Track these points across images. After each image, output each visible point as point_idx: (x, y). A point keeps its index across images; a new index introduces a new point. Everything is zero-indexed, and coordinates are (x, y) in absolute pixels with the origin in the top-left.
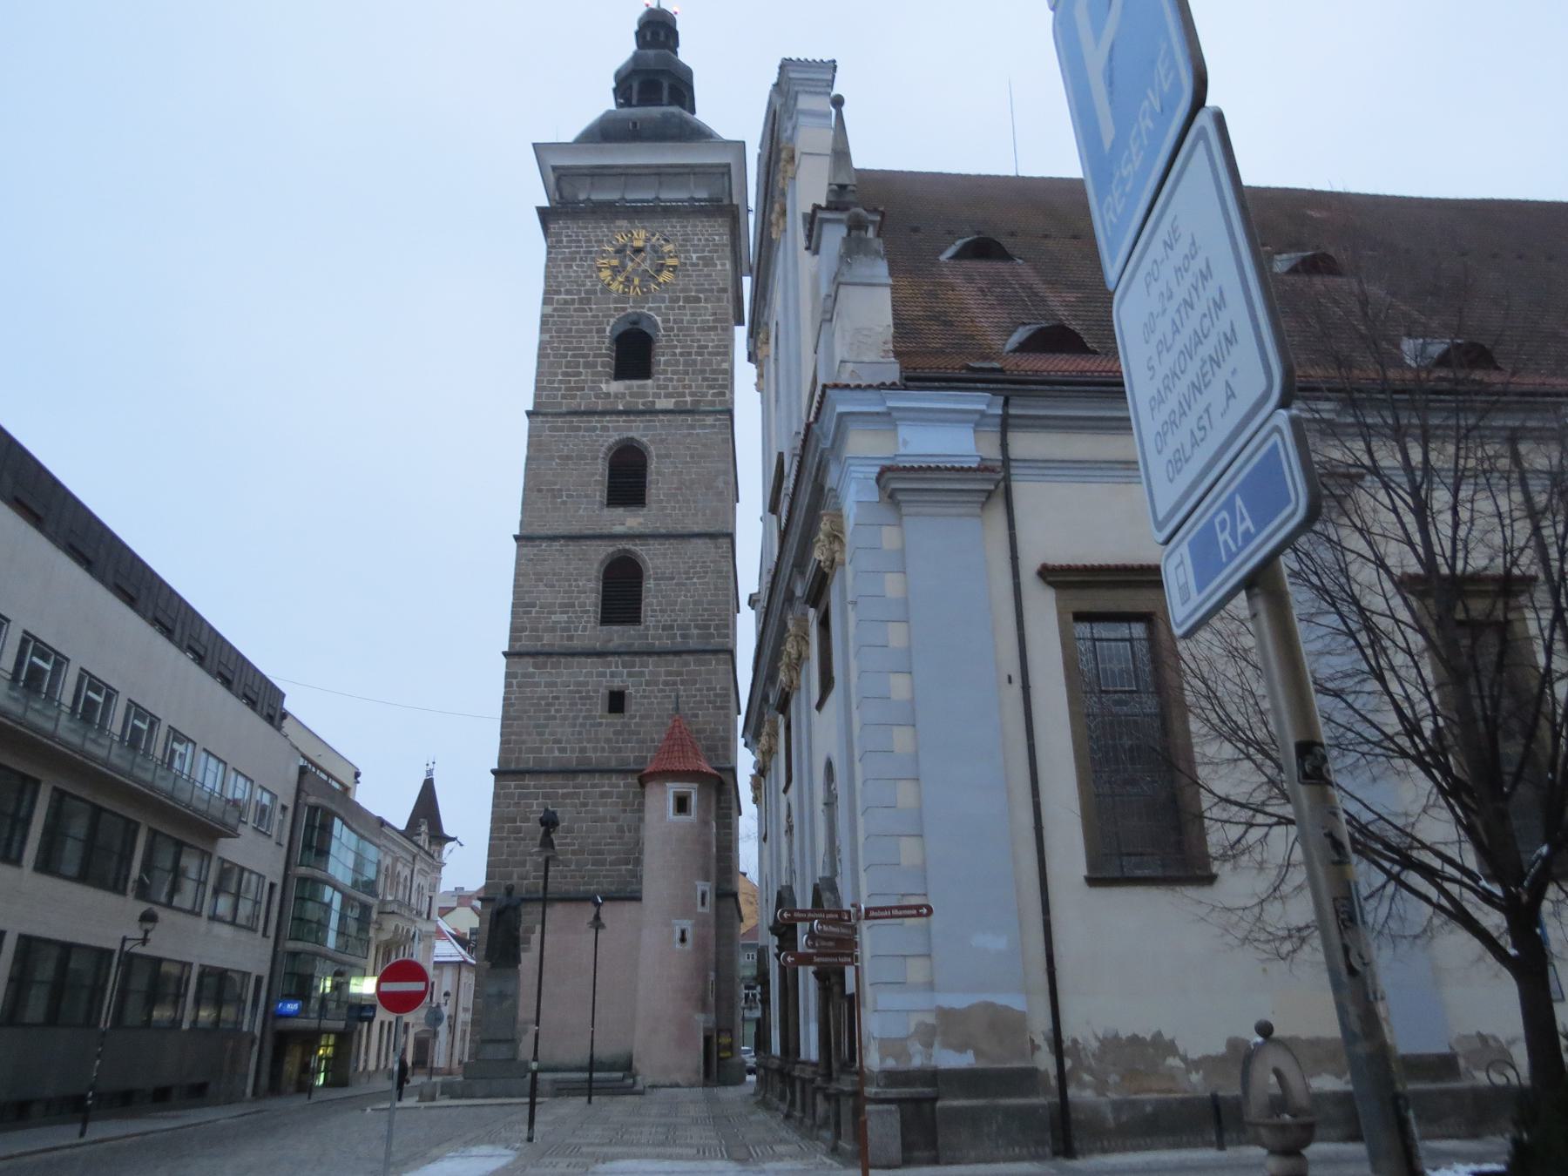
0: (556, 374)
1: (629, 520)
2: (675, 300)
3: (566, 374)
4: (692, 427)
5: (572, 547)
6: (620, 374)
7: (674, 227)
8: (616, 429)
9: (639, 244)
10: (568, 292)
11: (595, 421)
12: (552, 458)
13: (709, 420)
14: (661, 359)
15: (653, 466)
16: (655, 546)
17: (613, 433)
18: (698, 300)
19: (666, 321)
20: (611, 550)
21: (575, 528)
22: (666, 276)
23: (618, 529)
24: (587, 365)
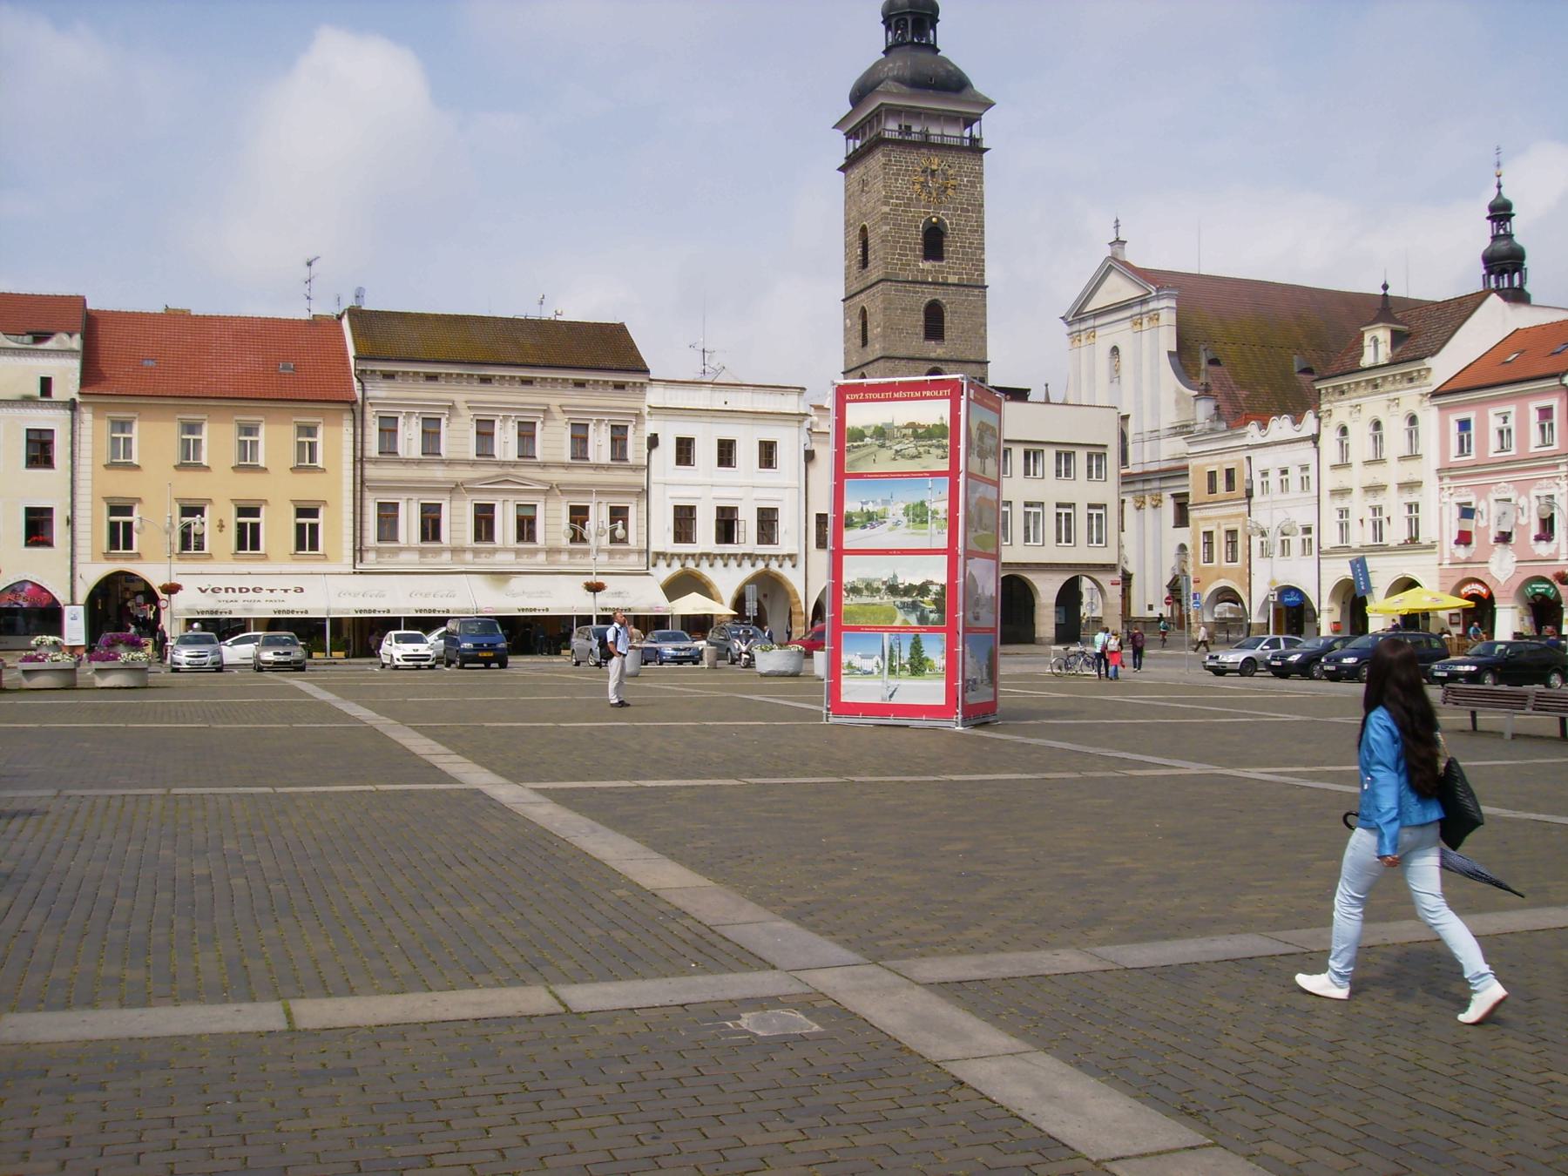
2: (955, 209)
5: (911, 364)
6: (927, 257)
9: (934, 167)
11: (918, 288)
13: (976, 292)
14: (950, 247)
15: (947, 317)
17: (928, 295)
21: (911, 353)
22: (950, 192)
23: (933, 355)
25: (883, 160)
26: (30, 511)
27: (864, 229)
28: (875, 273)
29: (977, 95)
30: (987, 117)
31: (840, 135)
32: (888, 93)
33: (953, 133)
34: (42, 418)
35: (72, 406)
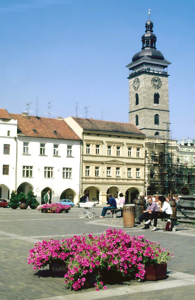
0: (147, 102)
1: (156, 127)
3: (148, 102)
4: (165, 113)
5: (151, 130)
6: (155, 103)
7: (160, 77)
8: (156, 112)
10: (148, 87)
12: (148, 116)
14: (160, 100)
16: (161, 131)
17: (156, 112)
18: (164, 91)
19: (161, 94)
20: (156, 132)
24: (151, 101)
25: (144, 77)
26: (4, 166)
27: (137, 95)
28: (141, 105)
29: (166, 61)
30: (169, 66)
31: (128, 69)
32: (146, 60)
33: (160, 70)
34: (7, 141)
35: (15, 138)
